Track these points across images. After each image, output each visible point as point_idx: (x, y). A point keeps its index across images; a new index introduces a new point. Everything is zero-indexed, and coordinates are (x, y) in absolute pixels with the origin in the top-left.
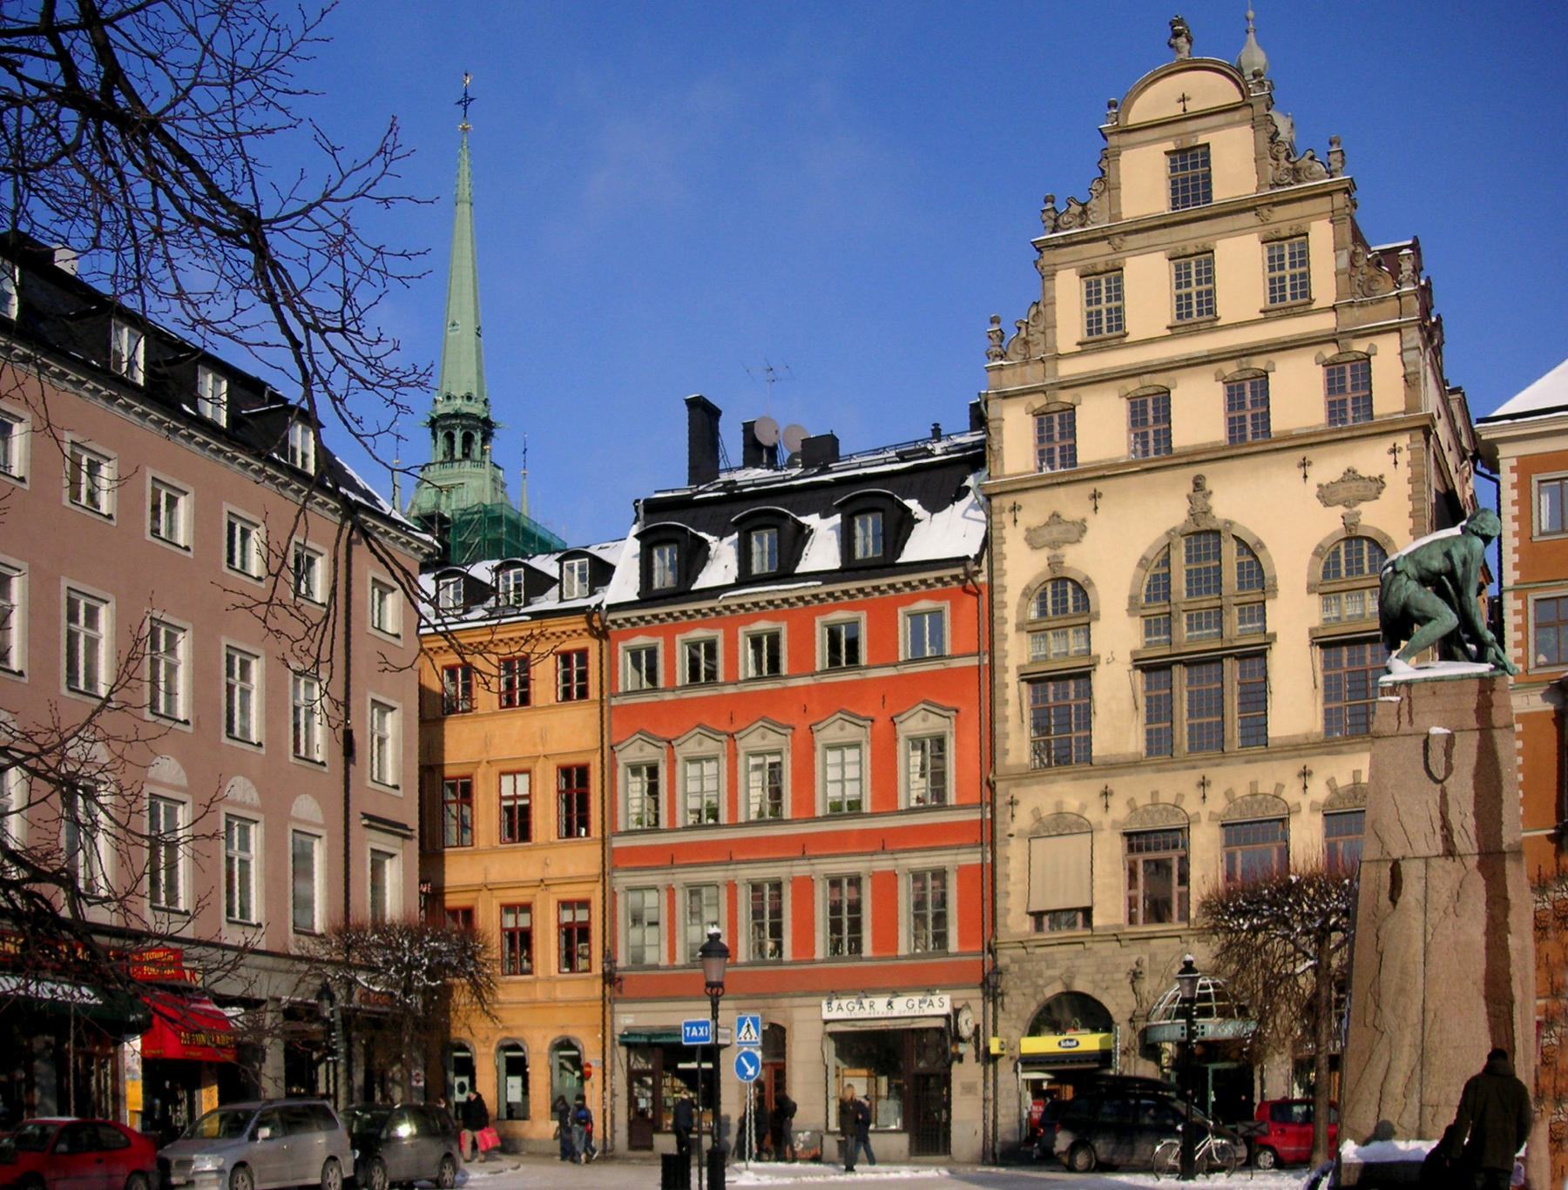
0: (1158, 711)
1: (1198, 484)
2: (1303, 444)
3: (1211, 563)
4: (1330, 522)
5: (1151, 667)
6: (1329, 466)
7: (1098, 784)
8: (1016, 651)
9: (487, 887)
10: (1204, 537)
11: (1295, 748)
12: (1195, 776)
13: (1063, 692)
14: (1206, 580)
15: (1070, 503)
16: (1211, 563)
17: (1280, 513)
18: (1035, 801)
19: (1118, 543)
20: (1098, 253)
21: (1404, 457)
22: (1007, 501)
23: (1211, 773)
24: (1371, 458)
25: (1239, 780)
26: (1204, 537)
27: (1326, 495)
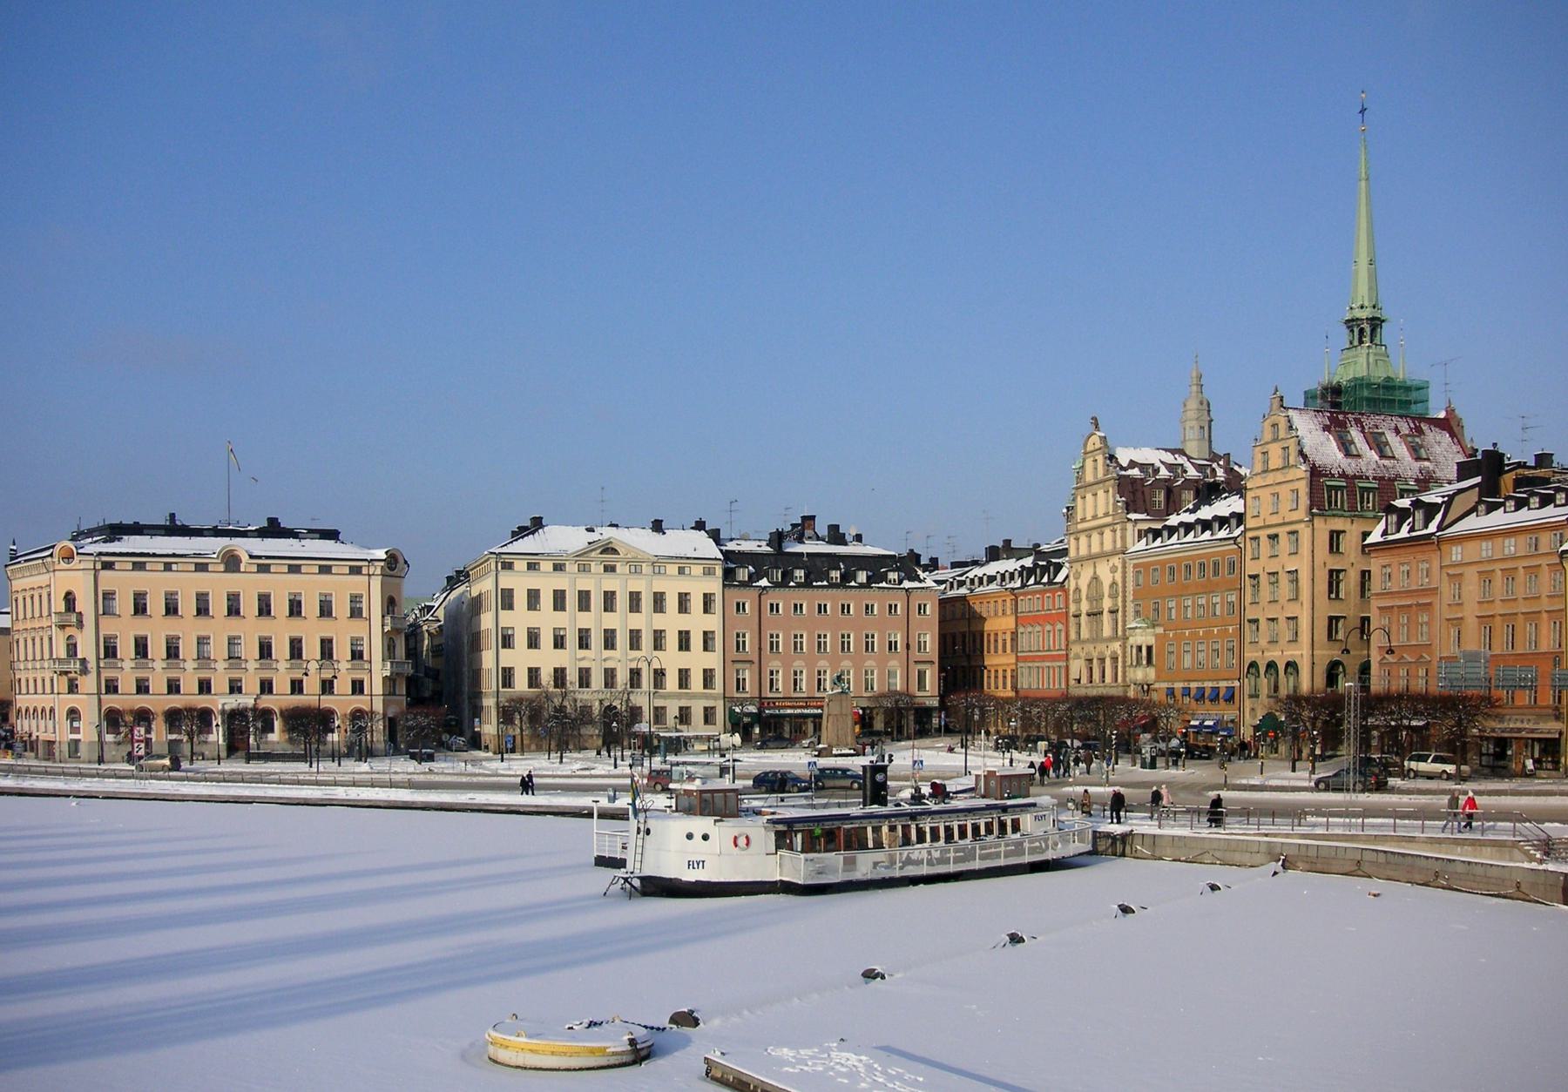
18: (1075, 649)
25: (1101, 647)
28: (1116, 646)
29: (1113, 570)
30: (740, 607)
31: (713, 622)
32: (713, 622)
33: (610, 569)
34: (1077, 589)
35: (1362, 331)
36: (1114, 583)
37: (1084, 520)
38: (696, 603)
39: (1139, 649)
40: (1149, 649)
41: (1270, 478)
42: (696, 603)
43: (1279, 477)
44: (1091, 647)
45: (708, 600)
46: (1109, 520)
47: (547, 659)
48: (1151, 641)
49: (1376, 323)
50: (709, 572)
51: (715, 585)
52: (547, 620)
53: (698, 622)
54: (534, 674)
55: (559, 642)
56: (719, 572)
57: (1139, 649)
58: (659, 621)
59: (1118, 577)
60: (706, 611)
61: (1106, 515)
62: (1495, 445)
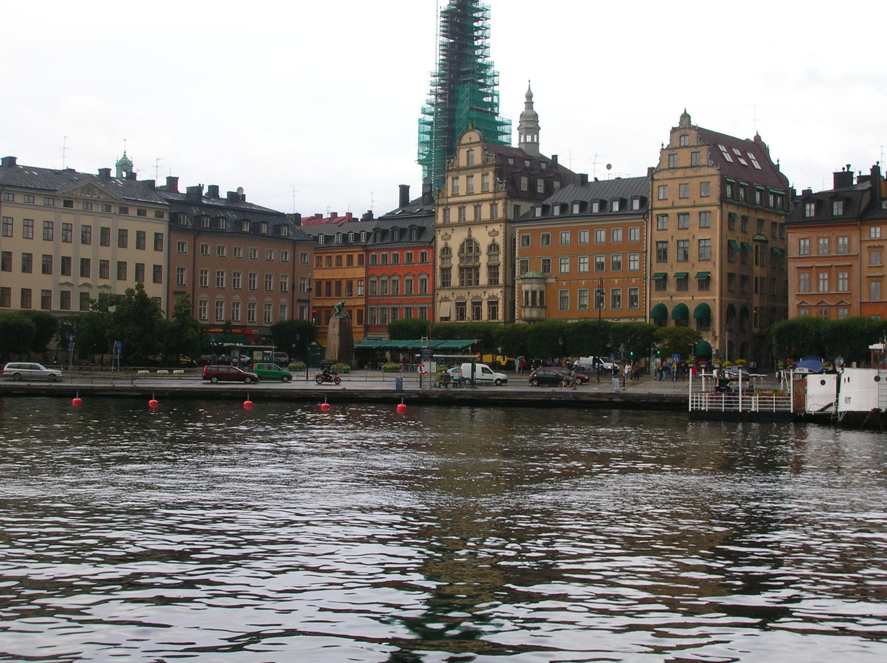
0: (461, 276)
2: (486, 223)
5: (461, 269)
6: (490, 228)
7: (451, 292)
8: (439, 262)
10: (470, 240)
11: (482, 287)
13: (446, 272)
14: (470, 249)
15: (449, 231)
16: (470, 246)
17: (482, 237)
18: (442, 294)
19: (456, 240)
23: (470, 291)
24: (498, 228)
25: (474, 292)
26: (470, 240)
28: (498, 292)
29: (494, 234)
30: (181, 245)
31: (160, 258)
32: (160, 258)
34: (447, 250)
36: (493, 247)
37: (455, 195)
38: (150, 241)
39: (534, 293)
40: (542, 293)
41: (679, 173)
42: (150, 241)
43: (690, 172)
44: (464, 293)
45: (158, 237)
46: (490, 196)
47: (37, 282)
48: (543, 288)
50: (159, 215)
51: (162, 228)
52: (39, 248)
53: (152, 258)
54: (26, 294)
55: (27, 267)
56: (166, 217)
57: (527, 293)
58: (123, 255)
59: (500, 240)
60: (156, 249)
61: (483, 192)
62: (848, 166)
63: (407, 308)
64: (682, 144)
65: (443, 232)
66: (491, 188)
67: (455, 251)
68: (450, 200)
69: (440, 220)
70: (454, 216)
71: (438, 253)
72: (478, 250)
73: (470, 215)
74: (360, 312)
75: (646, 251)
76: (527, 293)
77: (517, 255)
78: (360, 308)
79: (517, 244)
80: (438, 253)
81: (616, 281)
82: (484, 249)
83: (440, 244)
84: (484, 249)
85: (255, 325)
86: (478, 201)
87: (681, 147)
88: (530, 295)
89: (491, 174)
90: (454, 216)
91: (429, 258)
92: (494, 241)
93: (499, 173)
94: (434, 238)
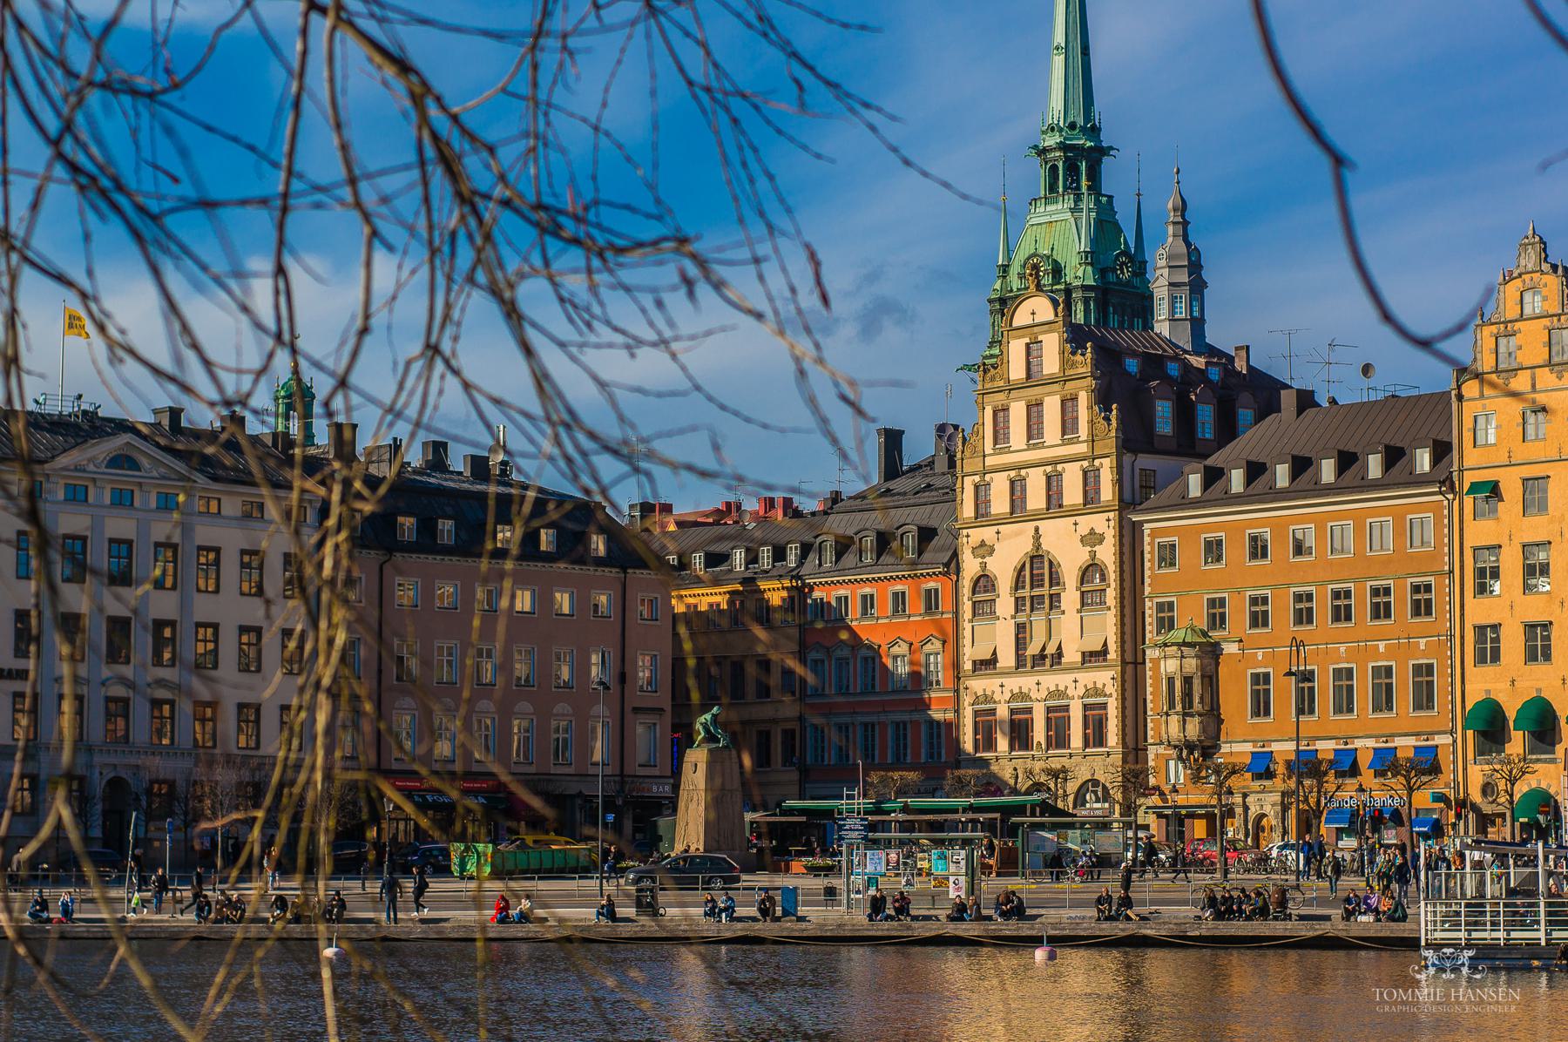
1: (1037, 529)
2: (1074, 512)
3: (1037, 573)
4: (1082, 556)
6: (1087, 523)
7: (998, 681)
9: (775, 721)
12: (1035, 679)
15: (987, 534)
16: (1037, 573)
17: (1066, 544)
20: (1000, 398)
21: (1112, 523)
22: (965, 532)
23: (1041, 678)
25: (1051, 680)
26: (1036, 558)
27: (1083, 540)
28: (1105, 678)
33: (122, 500)
34: (984, 582)
35: (1072, 169)
36: (1091, 570)
44: (1025, 682)
46: (1082, 448)
49: (1097, 155)
57: (1171, 681)
59: (1107, 554)
63: (866, 725)
64: (1528, 311)
65: (977, 535)
66: (1083, 431)
67: (1005, 584)
68: (989, 461)
69: (968, 510)
70: (1000, 503)
71: (966, 590)
72: (1055, 580)
73: (1036, 498)
74: (789, 735)
75: (1451, 572)
76: (1171, 681)
77: (1147, 590)
78: (789, 726)
79: (1147, 564)
80: (966, 590)
81: (1382, 646)
82: (1070, 577)
83: (970, 566)
84: (1070, 577)
85: (571, 770)
86: (1054, 462)
87: (1522, 318)
88: (1178, 684)
89: (1083, 398)
90: (1000, 503)
91: (945, 604)
92: (1093, 555)
93: (1103, 399)
94: (955, 555)
